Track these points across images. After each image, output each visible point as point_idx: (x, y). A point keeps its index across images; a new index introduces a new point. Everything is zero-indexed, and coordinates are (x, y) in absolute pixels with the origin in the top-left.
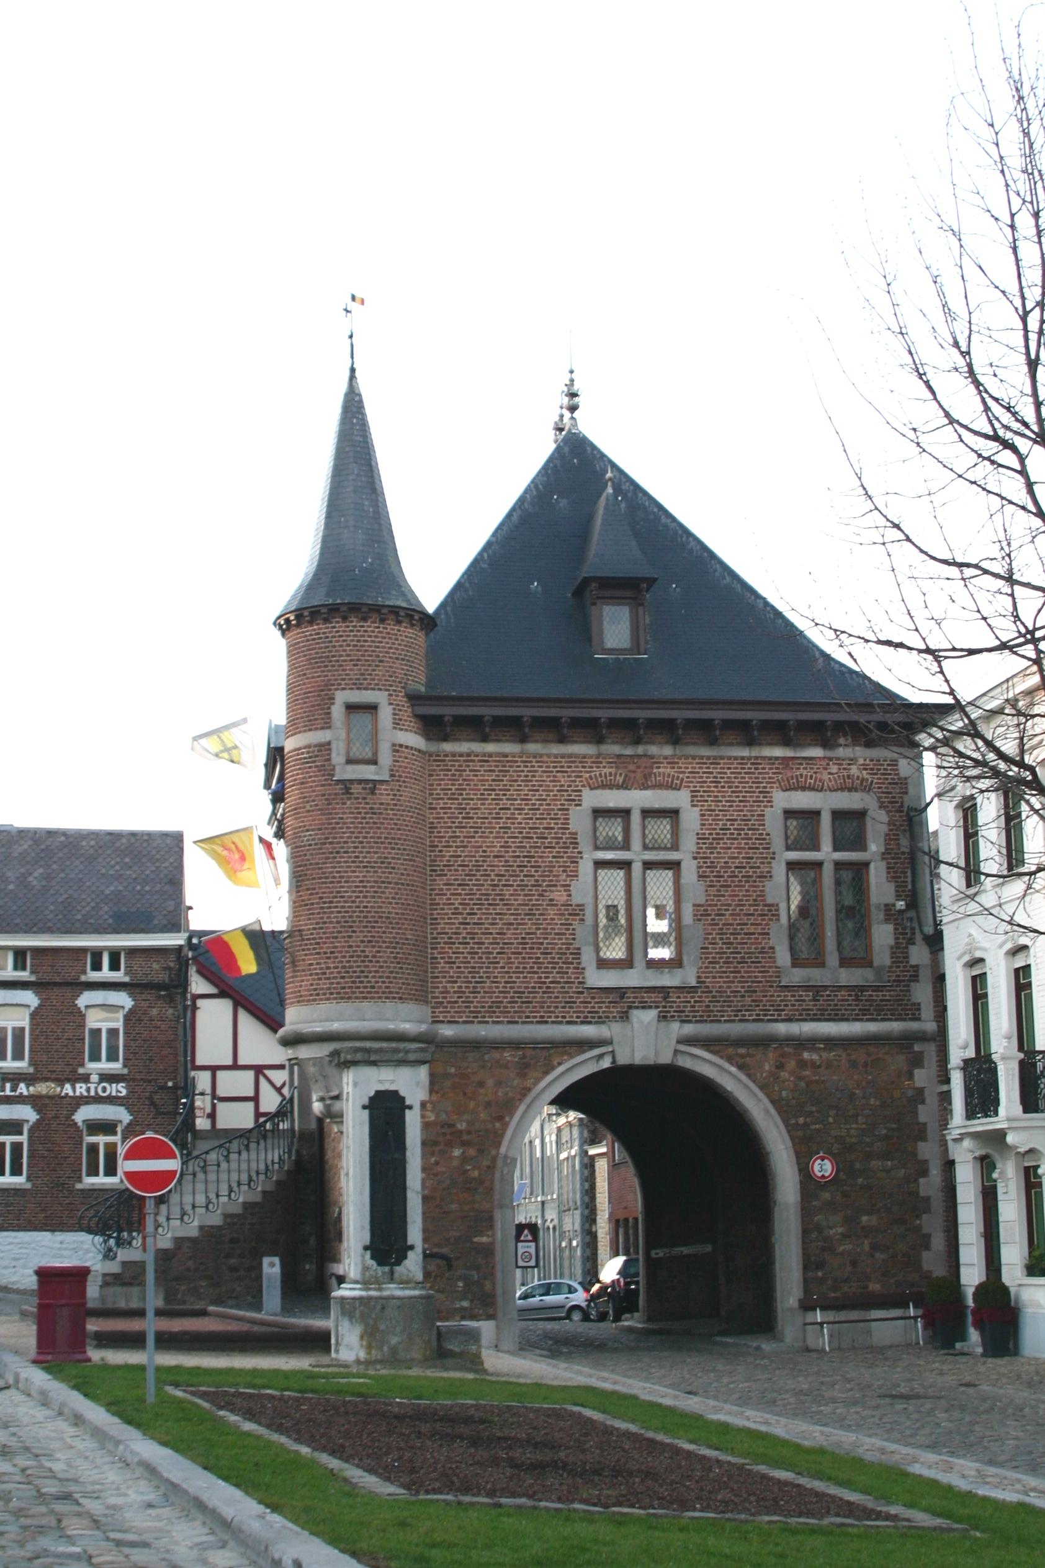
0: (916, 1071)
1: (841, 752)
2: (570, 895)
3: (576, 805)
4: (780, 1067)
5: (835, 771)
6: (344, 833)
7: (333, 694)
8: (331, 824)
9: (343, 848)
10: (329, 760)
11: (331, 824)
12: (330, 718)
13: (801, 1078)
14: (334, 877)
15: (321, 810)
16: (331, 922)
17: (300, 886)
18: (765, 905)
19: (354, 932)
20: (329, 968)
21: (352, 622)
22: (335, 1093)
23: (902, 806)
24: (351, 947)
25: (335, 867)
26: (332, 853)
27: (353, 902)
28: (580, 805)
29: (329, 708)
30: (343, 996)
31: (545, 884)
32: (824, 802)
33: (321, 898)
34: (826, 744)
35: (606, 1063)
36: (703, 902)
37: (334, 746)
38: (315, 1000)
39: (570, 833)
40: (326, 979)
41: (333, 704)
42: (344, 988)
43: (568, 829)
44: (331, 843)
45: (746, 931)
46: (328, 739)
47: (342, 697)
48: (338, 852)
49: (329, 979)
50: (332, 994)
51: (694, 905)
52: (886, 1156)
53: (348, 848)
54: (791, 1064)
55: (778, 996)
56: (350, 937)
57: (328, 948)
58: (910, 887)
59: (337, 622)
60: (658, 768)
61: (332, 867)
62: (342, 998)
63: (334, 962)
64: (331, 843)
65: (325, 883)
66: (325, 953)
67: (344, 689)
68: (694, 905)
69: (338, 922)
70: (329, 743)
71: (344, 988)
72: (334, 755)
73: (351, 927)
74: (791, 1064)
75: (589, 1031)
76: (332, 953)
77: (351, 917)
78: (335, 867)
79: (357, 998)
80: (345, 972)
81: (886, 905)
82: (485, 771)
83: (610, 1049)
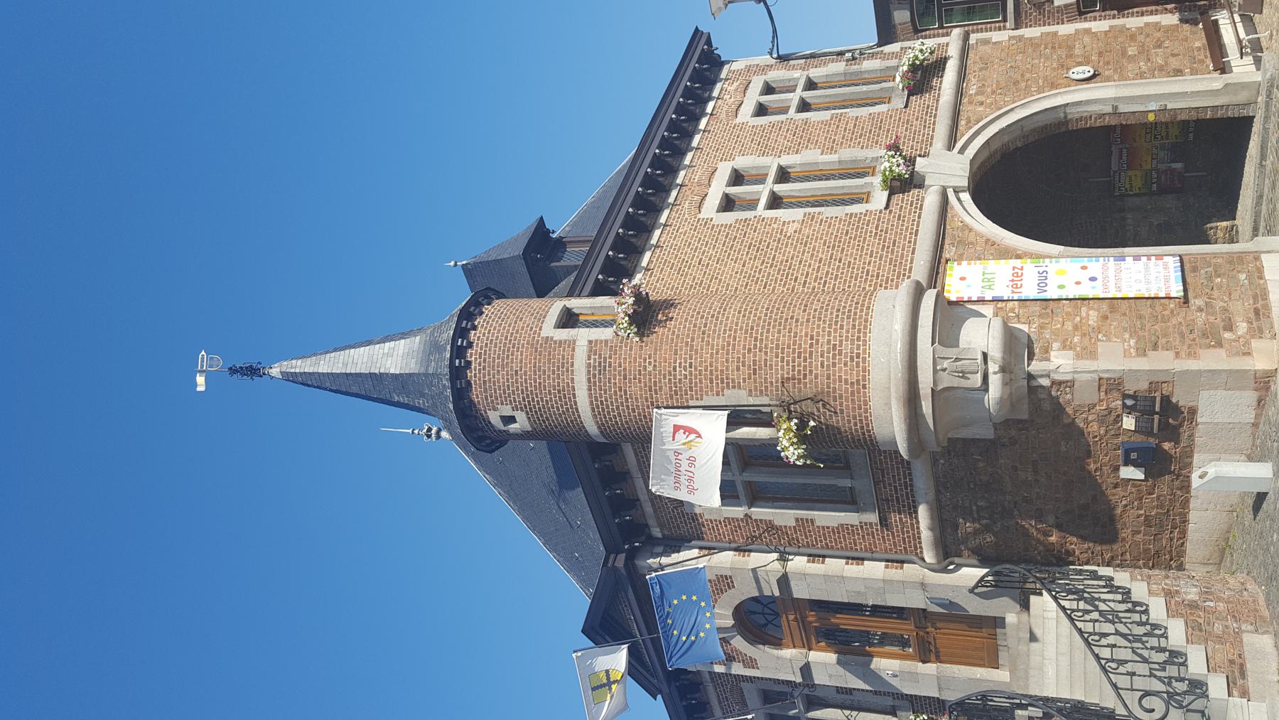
0: (993, 41)
1: (715, 94)
2: (794, 221)
3: (711, 221)
4: (982, 104)
5: (729, 96)
6: (685, 327)
7: (542, 338)
8: (672, 340)
9: (700, 328)
10: (606, 341)
11: (672, 340)
12: (565, 341)
13: (993, 92)
14: (729, 336)
15: (656, 350)
16: (778, 340)
17: (733, 381)
18: (831, 120)
19: (792, 317)
20: (829, 342)
21: (479, 322)
22: (980, 357)
23: (768, 66)
24: (808, 321)
25: (719, 335)
26: (703, 338)
27: (760, 318)
28: (712, 219)
29: (555, 342)
30: (861, 327)
31: (778, 236)
32: (754, 96)
33: (750, 350)
34: (710, 98)
35: (966, 197)
36: (820, 150)
37: (593, 338)
38: (864, 359)
39: (736, 223)
40: (841, 346)
41: (552, 338)
42: (854, 325)
43: (731, 224)
44: (693, 340)
45: (852, 128)
46: (586, 343)
47: (549, 329)
48: (704, 333)
49: (841, 342)
50: (859, 338)
51: (822, 154)
52: (1071, 48)
53: (701, 323)
54: (980, 98)
55: (915, 108)
56: (797, 321)
57: (805, 342)
58: (835, 57)
59: (475, 334)
60: (694, 179)
61: (718, 338)
62: (865, 327)
63: (823, 336)
64: (693, 340)
65: (734, 345)
66: (811, 345)
67: (540, 329)
68: (822, 154)
69: (779, 332)
70: (590, 342)
71: (854, 325)
72: (603, 338)
73: (787, 319)
74: (980, 98)
75: (931, 200)
76: (812, 338)
77: (775, 321)
78: (719, 335)
79: (867, 314)
80: (836, 325)
81: (847, 65)
82: (661, 274)
83: (951, 190)
